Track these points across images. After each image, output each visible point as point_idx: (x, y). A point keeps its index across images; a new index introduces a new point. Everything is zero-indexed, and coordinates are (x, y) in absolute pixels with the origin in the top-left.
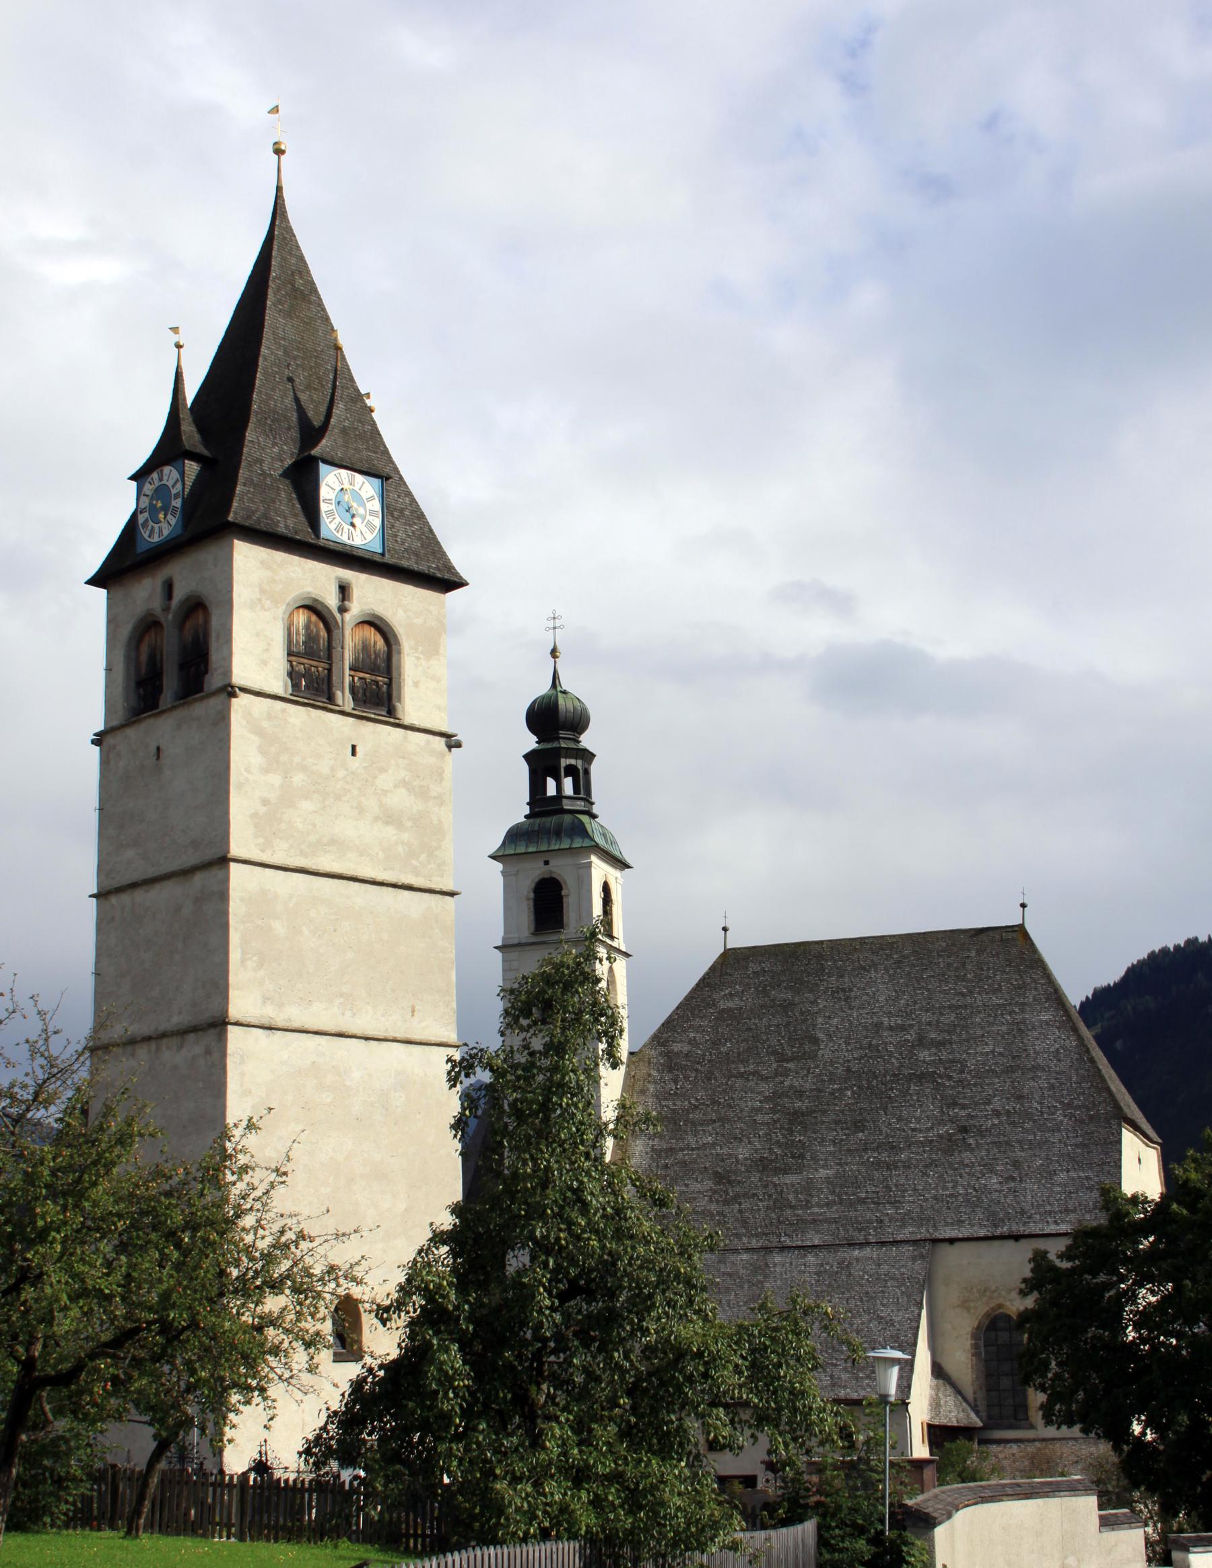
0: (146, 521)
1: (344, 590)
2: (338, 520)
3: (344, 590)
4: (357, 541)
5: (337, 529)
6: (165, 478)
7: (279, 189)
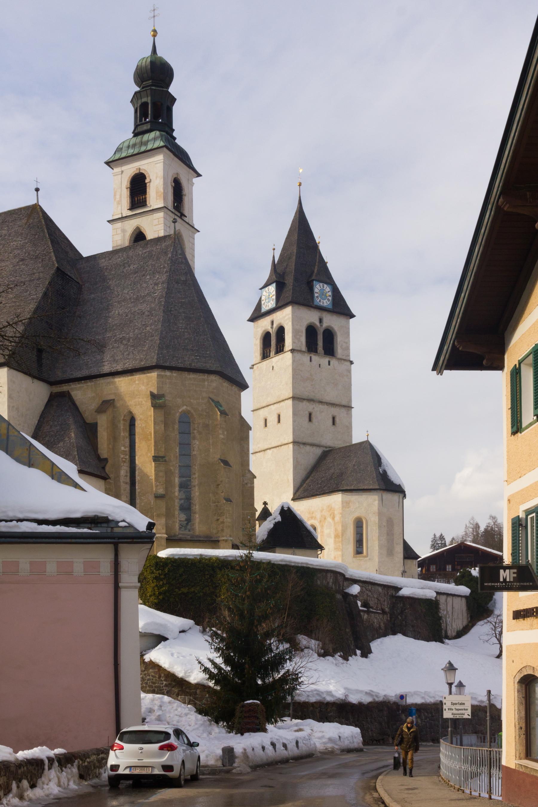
0: (264, 303)
1: (321, 321)
2: (320, 299)
3: (321, 321)
4: (325, 304)
5: (319, 302)
6: (270, 290)
7: (300, 197)
